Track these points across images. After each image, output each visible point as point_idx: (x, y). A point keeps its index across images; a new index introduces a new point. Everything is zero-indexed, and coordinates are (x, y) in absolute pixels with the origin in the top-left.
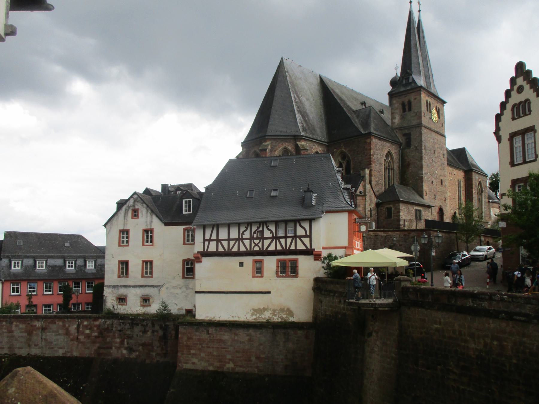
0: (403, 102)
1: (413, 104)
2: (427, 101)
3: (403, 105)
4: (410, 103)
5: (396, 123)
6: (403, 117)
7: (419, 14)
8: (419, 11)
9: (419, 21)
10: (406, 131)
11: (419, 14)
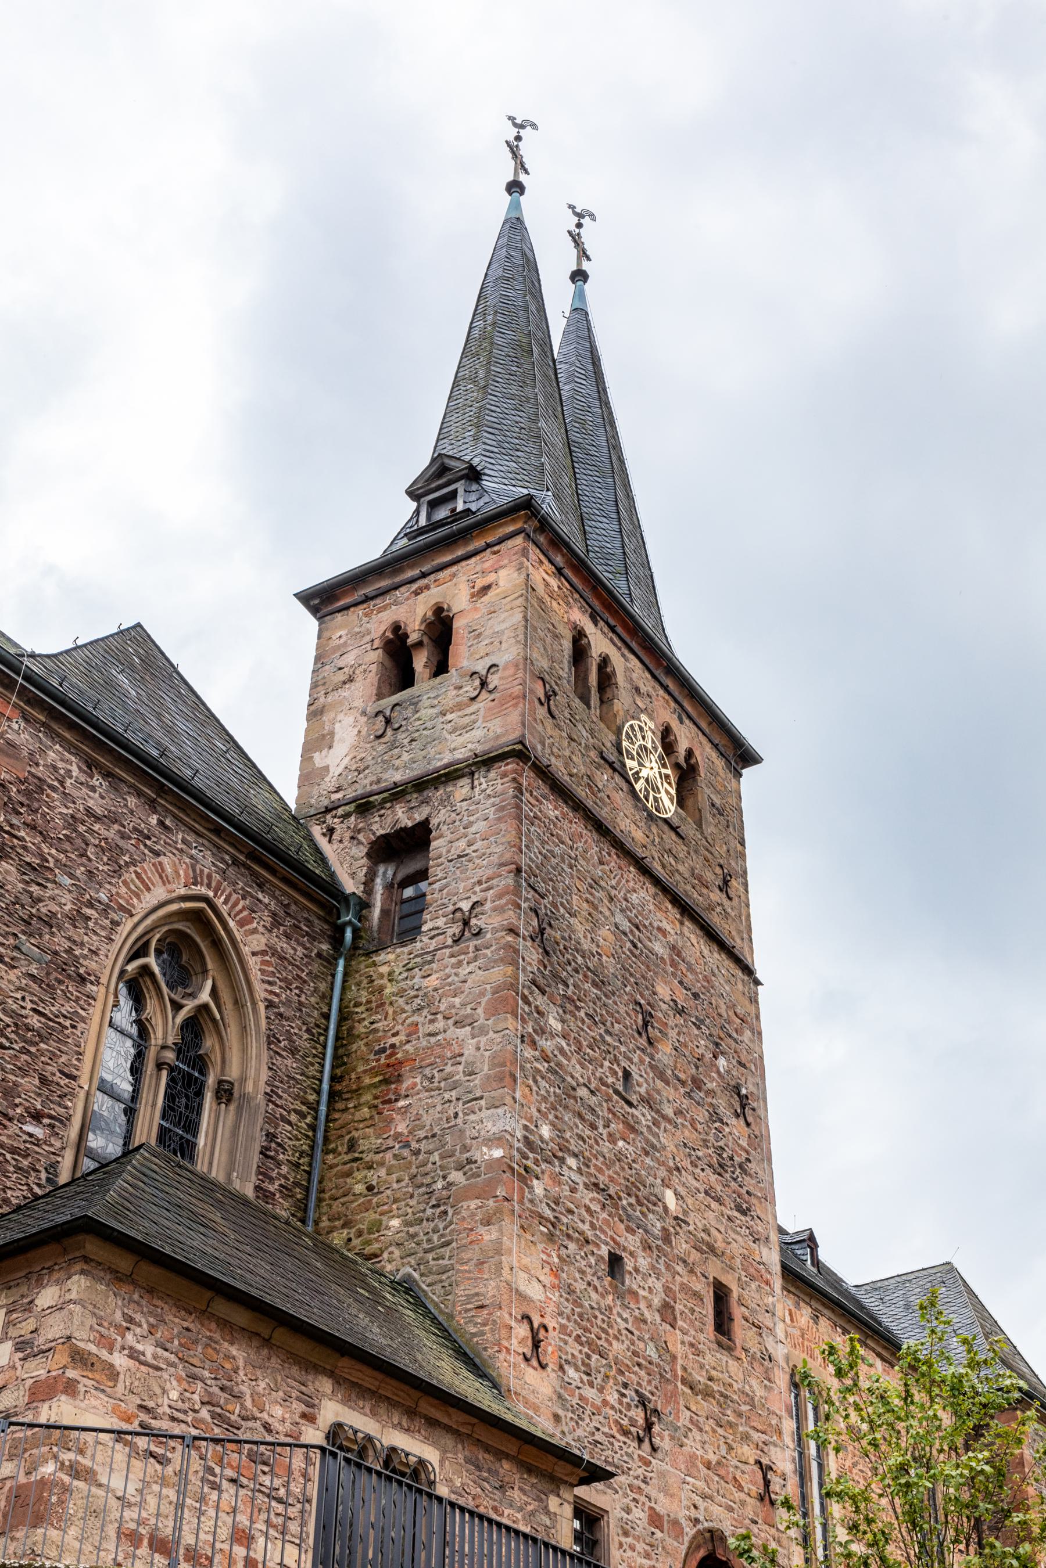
0: (396, 628)
1: (458, 624)
2: (579, 637)
3: (397, 651)
4: (441, 628)
5: (335, 771)
6: (387, 724)
7: (580, 295)
8: (579, 276)
9: (580, 314)
10: (402, 816)
11: (580, 295)
